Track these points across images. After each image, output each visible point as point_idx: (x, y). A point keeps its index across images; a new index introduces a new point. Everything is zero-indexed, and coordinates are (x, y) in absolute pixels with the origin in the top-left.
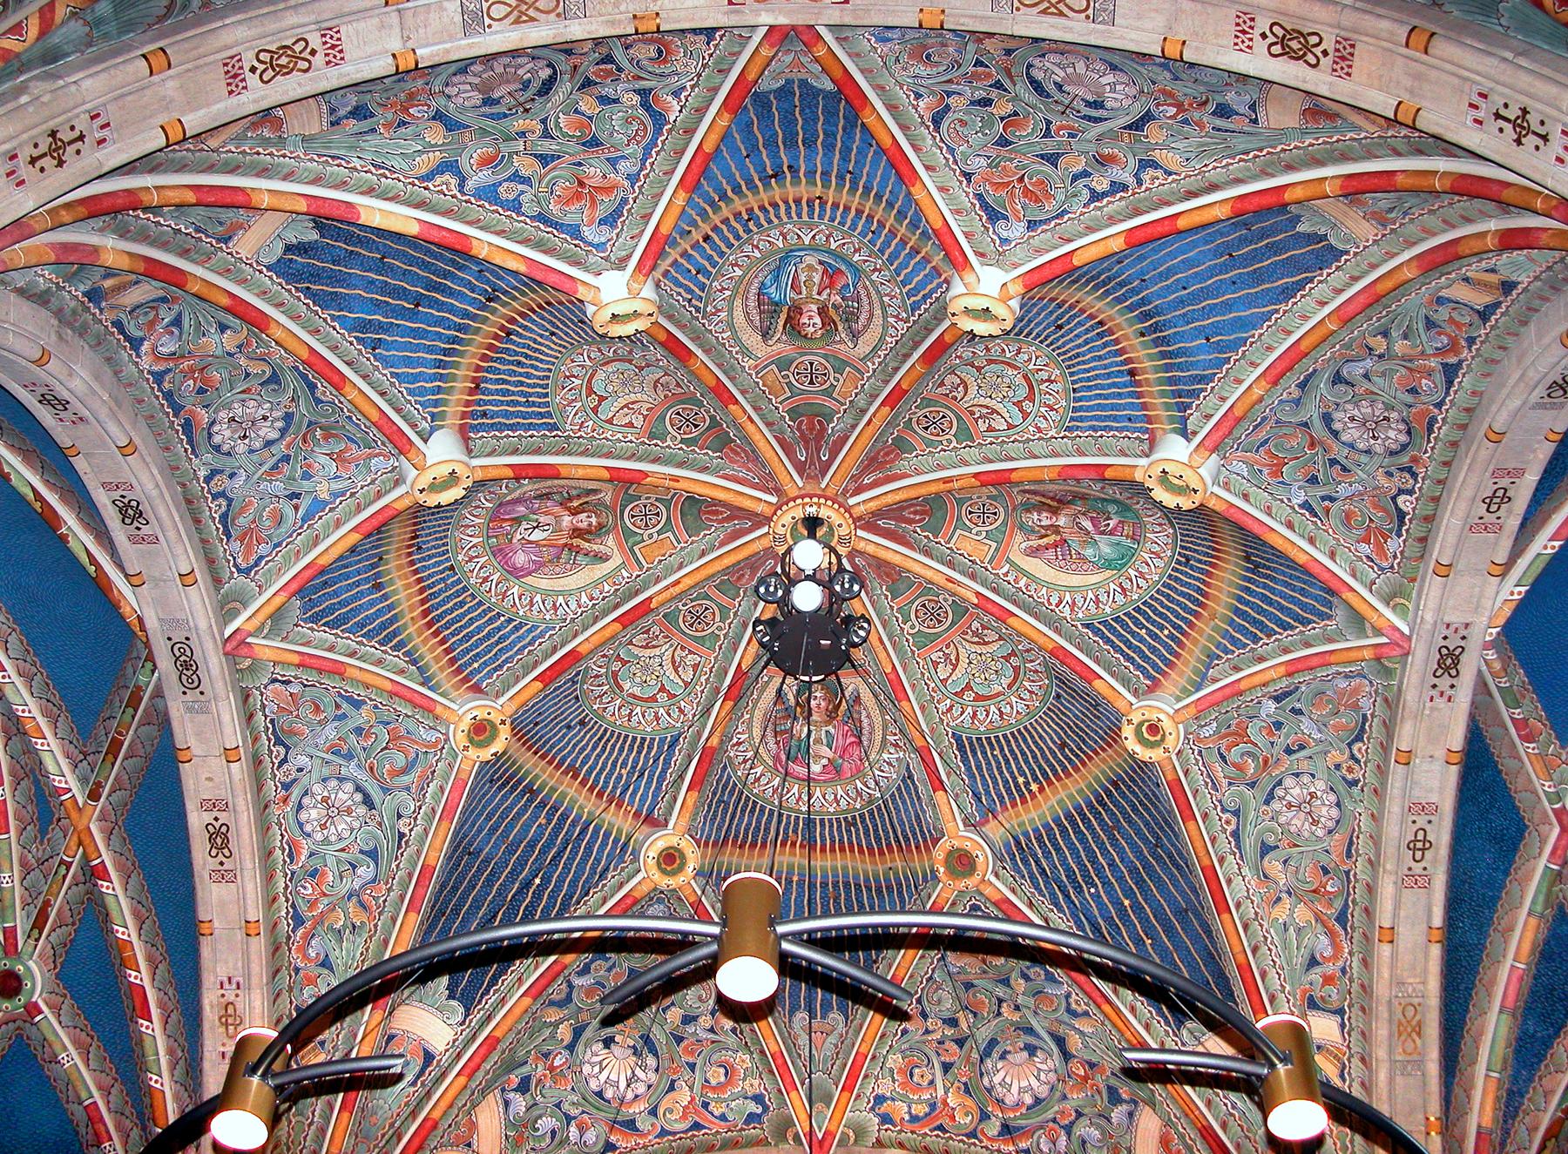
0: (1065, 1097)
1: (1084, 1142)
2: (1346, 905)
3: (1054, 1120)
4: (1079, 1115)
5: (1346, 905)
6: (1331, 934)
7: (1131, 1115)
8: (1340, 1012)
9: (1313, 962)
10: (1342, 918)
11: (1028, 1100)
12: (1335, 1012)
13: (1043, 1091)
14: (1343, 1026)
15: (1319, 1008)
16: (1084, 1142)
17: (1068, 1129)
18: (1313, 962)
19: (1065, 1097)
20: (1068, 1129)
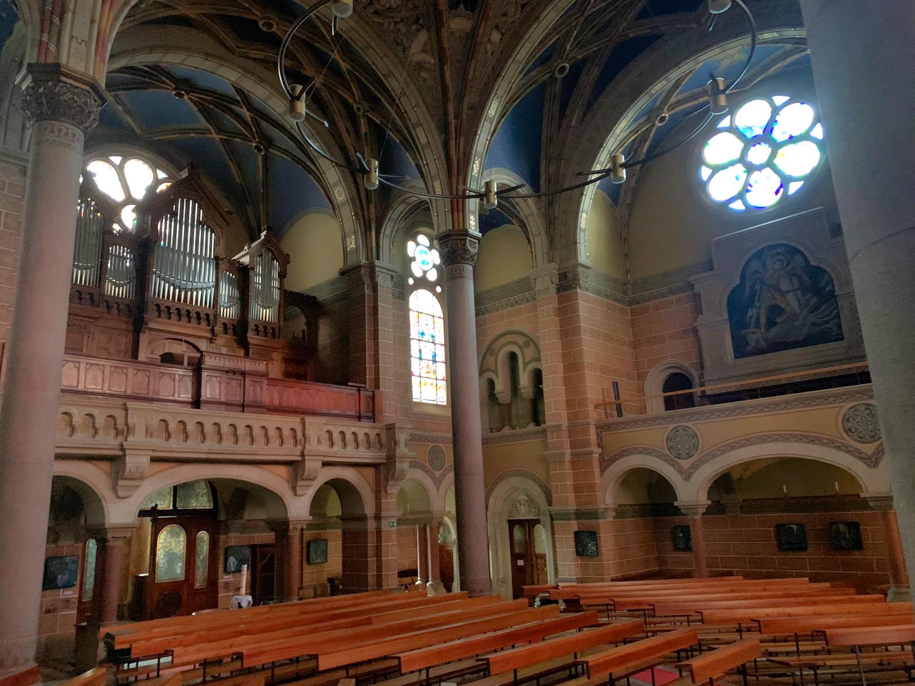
0: (400, 12)
1: (399, 30)
2: (527, 3)
3: (393, 18)
4: (402, 21)
5: (527, 3)
6: (516, 9)
7: (419, 30)
8: (503, 34)
9: (505, 15)
10: (523, 6)
11: (388, 6)
12: (501, 33)
13: (394, 6)
14: (501, 39)
15: (498, 30)
16: (399, 30)
17: (396, 23)
18: (505, 15)
19: (400, 12)
20: (396, 23)
